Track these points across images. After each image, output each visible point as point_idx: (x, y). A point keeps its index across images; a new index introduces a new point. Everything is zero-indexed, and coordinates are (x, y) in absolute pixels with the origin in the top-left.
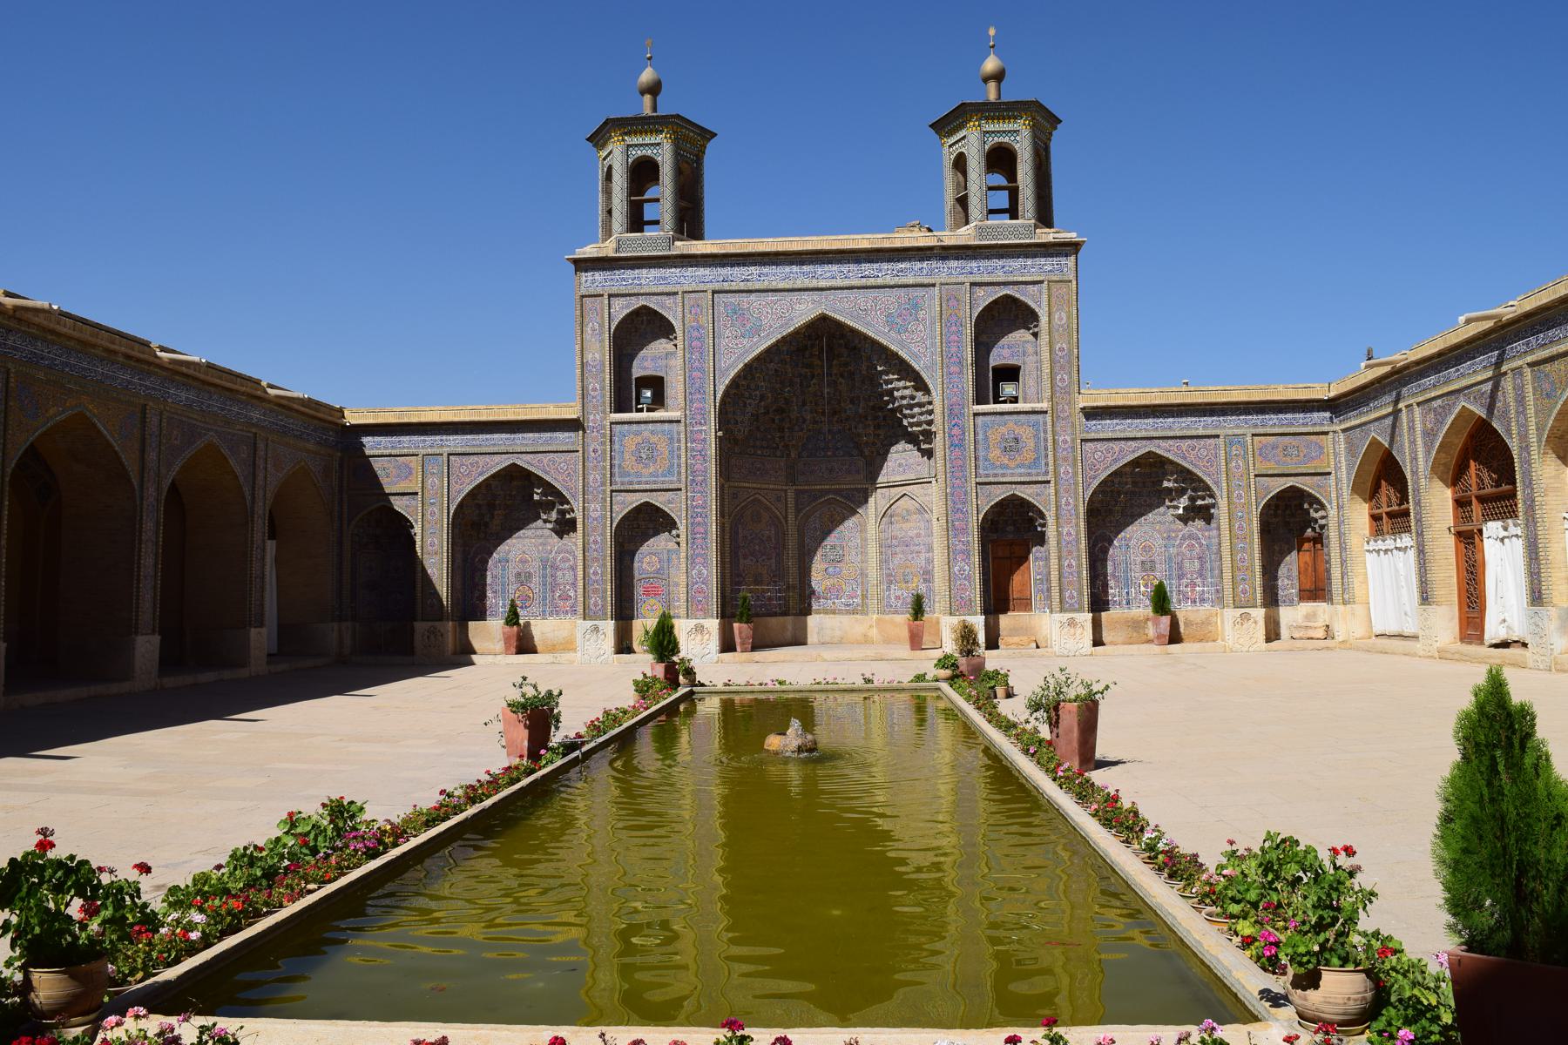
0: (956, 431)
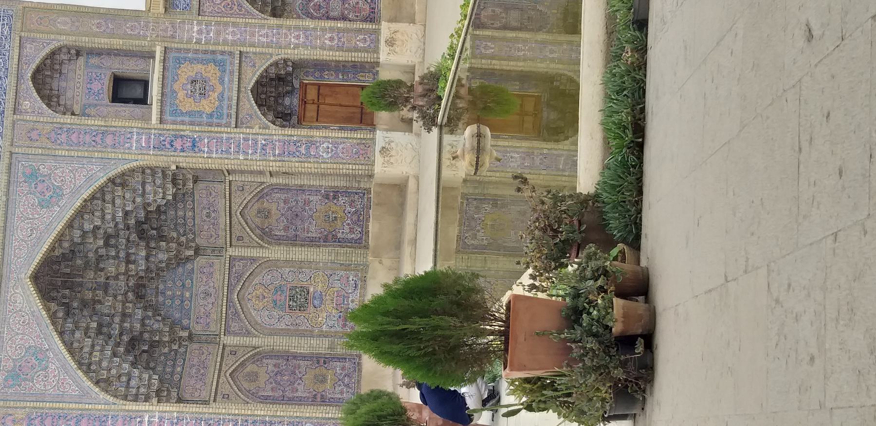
0: (178, 144)
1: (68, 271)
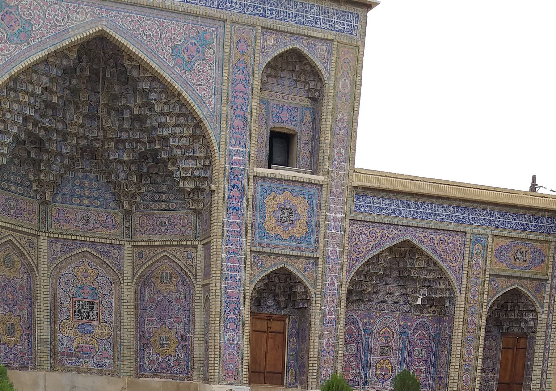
1: (108, 76)
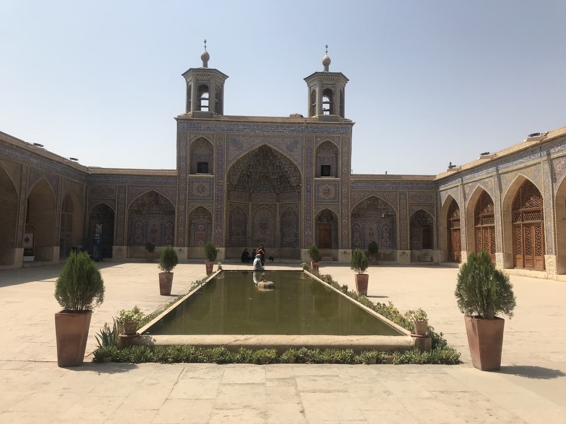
0: (308, 186)
